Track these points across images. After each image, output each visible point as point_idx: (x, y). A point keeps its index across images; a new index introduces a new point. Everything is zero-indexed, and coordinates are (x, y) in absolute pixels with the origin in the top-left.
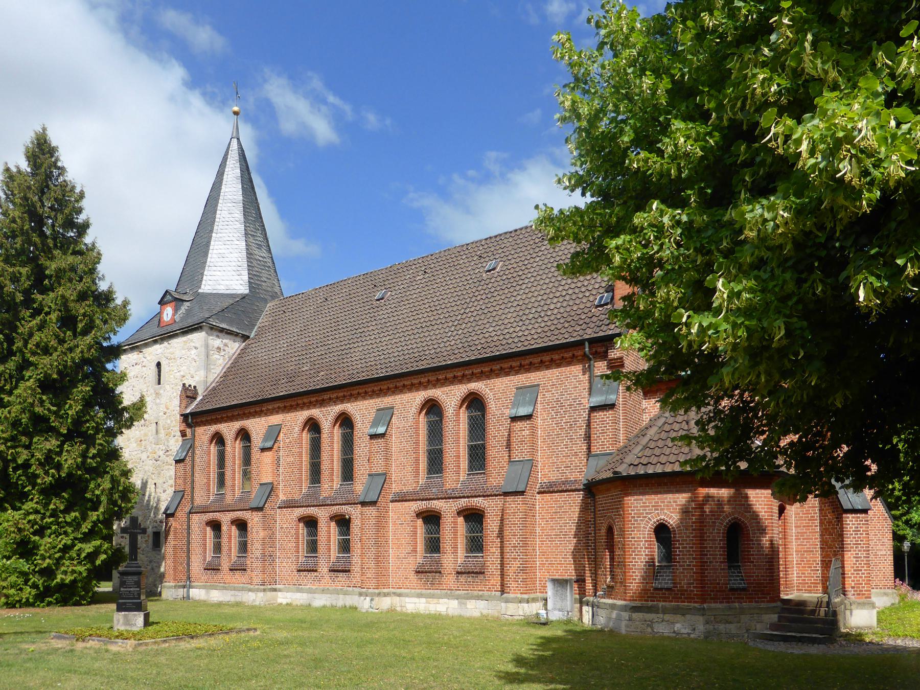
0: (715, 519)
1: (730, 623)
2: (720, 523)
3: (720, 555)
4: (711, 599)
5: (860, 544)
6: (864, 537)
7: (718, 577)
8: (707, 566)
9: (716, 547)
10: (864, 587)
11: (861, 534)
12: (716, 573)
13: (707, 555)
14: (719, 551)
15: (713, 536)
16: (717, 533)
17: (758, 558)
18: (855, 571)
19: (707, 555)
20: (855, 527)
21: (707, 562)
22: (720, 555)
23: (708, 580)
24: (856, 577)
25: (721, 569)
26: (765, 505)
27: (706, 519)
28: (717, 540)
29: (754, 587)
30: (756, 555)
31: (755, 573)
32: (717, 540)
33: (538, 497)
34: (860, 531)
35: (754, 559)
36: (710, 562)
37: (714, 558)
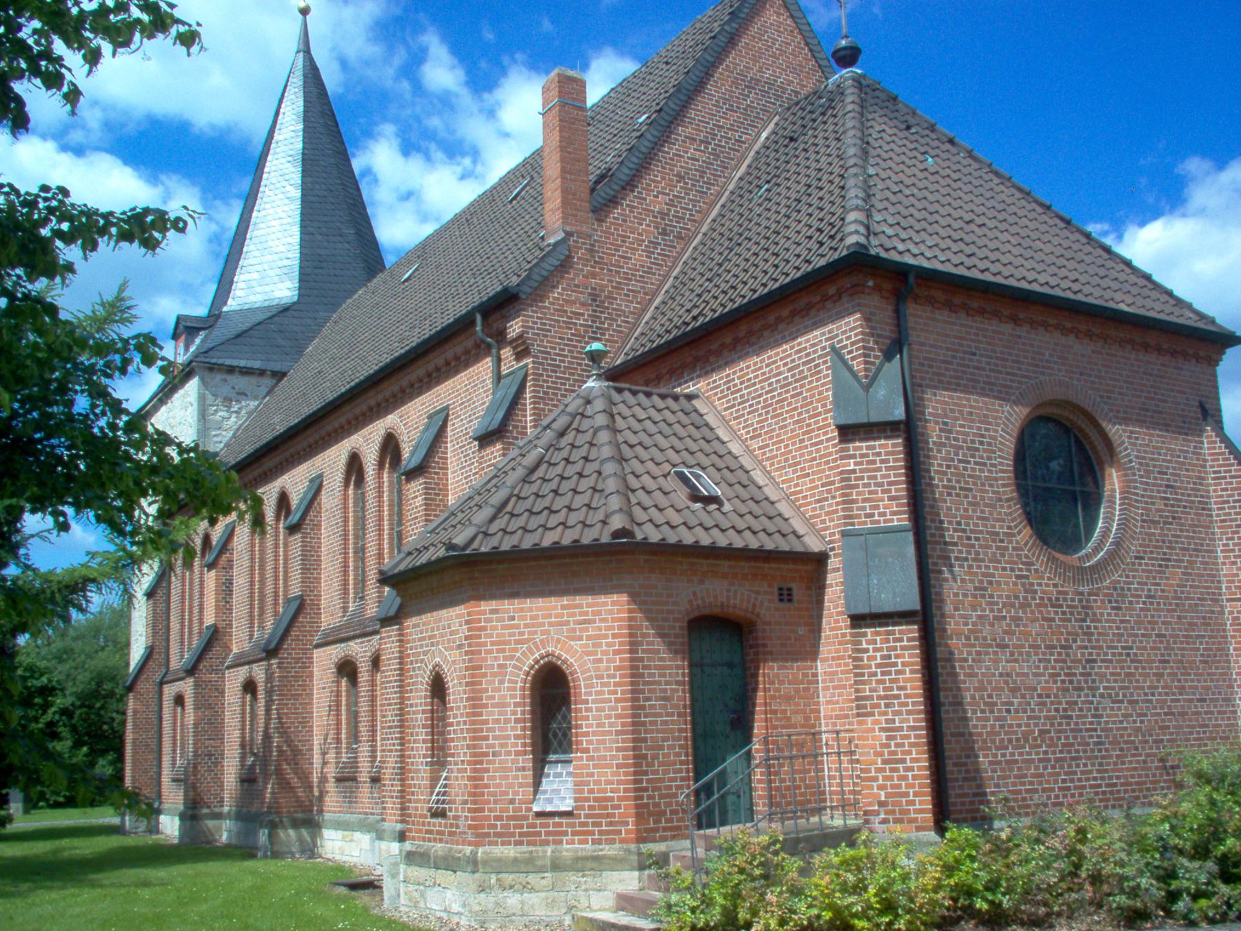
0: (505, 658)
1: (532, 890)
2: (515, 667)
3: (517, 737)
4: (497, 835)
5: (897, 697)
6: (905, 680)
7: (511, 785)
8: (489, 762)
9: (507, 721)
10: (912, 803)
11: (898, 672)
12: (507, 777)
13: (486, 738)
14: (513, 729)
15: (501, 697)
16: (509, 689)
17: (599, 742)
18: (884, 762)
19: (486, 738)
20: (883, 657)
21: (486, 754)
22: (517, 737)
23: (490, 794)
24: (890, 778)
25: (518, 769)
26: (614, 620)
27: (486, 659)
28: (508, 705)
29: (591, 808)
30: (595, 733)
31: (592, 775)
32: (508, 705)
33: (776, 586)
34: (895, 664)
35: (589, 742)
36: (494, 754)
37: (502, 745)
